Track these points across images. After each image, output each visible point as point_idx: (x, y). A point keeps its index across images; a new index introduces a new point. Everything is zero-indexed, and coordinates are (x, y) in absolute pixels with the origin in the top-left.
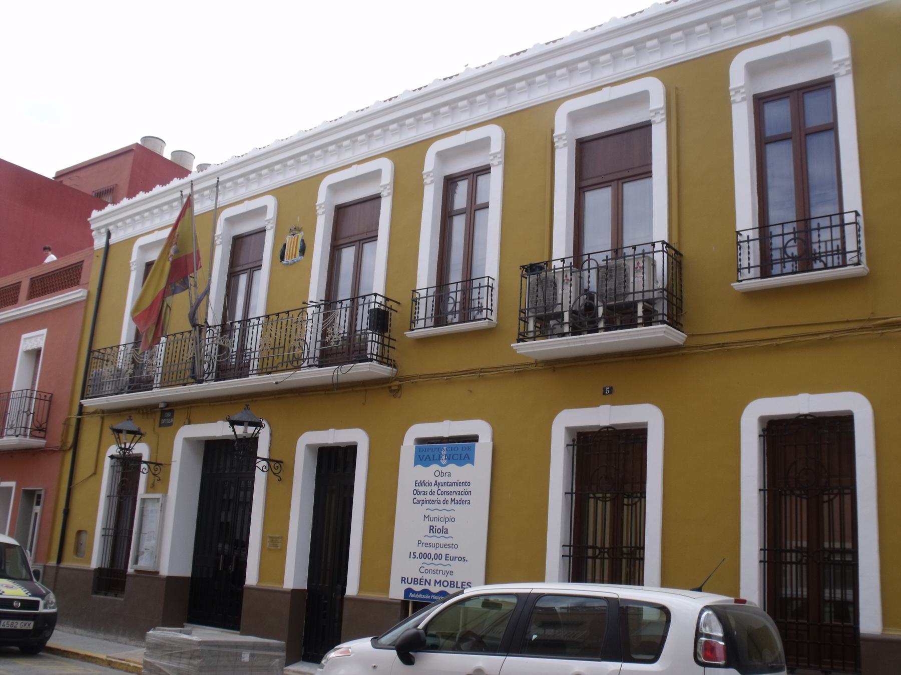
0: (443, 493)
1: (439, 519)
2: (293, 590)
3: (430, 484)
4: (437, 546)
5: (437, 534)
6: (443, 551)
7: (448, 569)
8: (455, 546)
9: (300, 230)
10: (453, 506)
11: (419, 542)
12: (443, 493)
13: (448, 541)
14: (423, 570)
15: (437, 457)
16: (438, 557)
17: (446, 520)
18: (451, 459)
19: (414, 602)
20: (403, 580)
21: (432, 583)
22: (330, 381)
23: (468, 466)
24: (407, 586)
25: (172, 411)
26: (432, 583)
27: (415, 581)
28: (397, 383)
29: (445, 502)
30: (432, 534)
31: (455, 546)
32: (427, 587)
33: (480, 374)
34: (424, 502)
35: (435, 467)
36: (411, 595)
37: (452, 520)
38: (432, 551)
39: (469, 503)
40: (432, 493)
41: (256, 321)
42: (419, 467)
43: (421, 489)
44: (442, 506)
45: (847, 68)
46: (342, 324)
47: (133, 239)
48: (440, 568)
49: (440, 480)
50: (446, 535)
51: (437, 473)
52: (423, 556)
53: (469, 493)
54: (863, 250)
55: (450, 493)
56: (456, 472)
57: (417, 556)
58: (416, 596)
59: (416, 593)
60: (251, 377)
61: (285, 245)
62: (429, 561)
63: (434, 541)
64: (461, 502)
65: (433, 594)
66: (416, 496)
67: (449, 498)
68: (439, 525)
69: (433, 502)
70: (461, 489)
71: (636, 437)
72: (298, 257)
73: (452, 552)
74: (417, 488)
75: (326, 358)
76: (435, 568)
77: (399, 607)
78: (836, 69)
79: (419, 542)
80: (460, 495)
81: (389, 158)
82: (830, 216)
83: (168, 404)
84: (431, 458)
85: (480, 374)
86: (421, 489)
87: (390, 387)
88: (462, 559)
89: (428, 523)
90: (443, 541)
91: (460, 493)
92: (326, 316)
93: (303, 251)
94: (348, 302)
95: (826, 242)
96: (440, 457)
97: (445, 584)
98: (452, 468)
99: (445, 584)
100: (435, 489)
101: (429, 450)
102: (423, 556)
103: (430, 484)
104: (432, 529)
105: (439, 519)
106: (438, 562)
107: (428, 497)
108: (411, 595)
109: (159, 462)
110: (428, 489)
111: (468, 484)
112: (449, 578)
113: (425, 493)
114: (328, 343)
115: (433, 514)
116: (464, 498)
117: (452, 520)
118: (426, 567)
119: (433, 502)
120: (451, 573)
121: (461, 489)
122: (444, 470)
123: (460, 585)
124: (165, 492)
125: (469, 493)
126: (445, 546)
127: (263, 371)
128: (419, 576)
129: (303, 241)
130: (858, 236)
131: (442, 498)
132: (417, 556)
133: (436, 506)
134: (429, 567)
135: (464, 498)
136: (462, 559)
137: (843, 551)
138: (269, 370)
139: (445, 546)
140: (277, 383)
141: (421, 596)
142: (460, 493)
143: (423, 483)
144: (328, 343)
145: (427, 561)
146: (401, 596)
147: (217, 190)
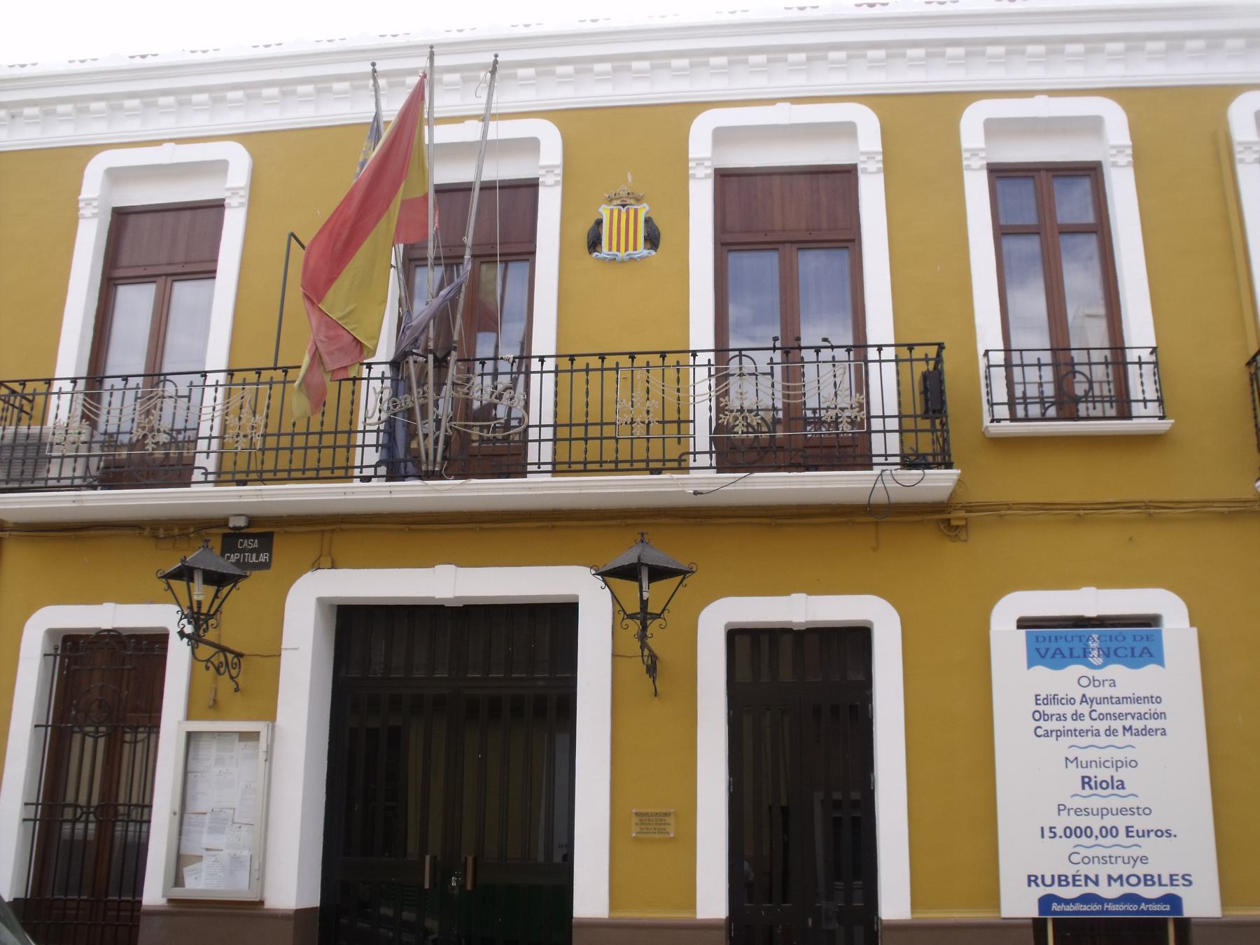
0: (1103, 717)
1: (1101, 764)
2: (299, 912)
3: (1071, 701)
4: (1102, 812)
5: (1100, 791)
6: (1121, 822)
7: (1135, 852)
8: (1147, 811)
9: (638, 200)
10: (1129, 739)
11: (1061, 808)
12: (1103, 717)
13: (1130, 803)
14: (1075, 858)
15: (1077, 653)
16: (1111, 832)
17: (1117, 765)
18: (1110, 656)
19: (1054, 920)
20: (1032, 880)
21: (1103, 880)
22: (862, 499)
23: (1152, 668)
24: (1043, 891)
25: (266, 541)
26: (1103, 880)
27: (1062, 880)
28: (962, 514)
29: (1111, 732)
30: (1088, 791)
31: (1147, 811)
32: (1091, 889)
33: (1149, 511)
34: (1060, 734)
35: (1076, 670)
36: (1055, 907)
37: (1133, 764)
38: (1095, 823)
39: (1164, 733)
40: (1077, 716)
41: (119, 383)
42: (1041, 671)
43: (1050, 709)
44: (1103, 740)
45: (1126, 158)
46: (207, 411)
47: (89, 151)
48: (1115, 852)
49: (1091, 692)
50: (1121, 792)
51: (1084, 682)
52: (1070, 832)
53: (1162, 715)
54: (985, 407)
55: (1120, 716)
56: (1125, 679)
57: (1060, 832)
58: (1069, 908)
59: (1067, 902)
60: (531, 478)
61: (599, 223)
62: (1092, 841)
63: (1095, 803)
64: (1147, 732)
65: (1108, 901)
66: (1041, 723)
67: (1117, 725)
68: (1103, 774)
69: (1082, 733)
70: (1143, 708)
71: (856, 640)
72: (642, 251)
73: (1139, 823)
74: (1041, 708)
75: (733, 453)
76: (1107, 852)
77: (1031, 932)
78: (1113, 156)
79: (1061, 808)
80: (1146, 720)
81: (558, 125)
82: (1088, 349)
83: (252, 520)
84: (1067, 653)
85: (1149, 511)
86: (1050, 709)
87: (949, 520)
88: (1160, 833)
89: (1076, 773)
90: (1115, 803)
91: (1141, 717)
92: (787, 375)
93: (653, 240)
94: (222, 378)
95: (1101, 383)
96: (1086, 653)
97: (1133, 880)
98: (1116, 671)
99: (1133, 880)
100: (1084, 709)
101: (1053, 638)
102: (1070, 832)
103: (1071, 701)
104: (1086, 782)
105: (1101, 764)
106: (1109, 840)
107: (1070, 724)
108: (1055, 907)
109: (224, 643)
110: (1068, 710)
111: (1159, 700)
112: (1141, 870)
113: (1061, 717)
114: (731, 429)
115: (1084, 756)
116: (1152, 724)
117: (1133, 764)
118: (1084, 852)
119: (1082, 733)
120: (1143, 860)
121: (1143, 708)
122: (1099, 674)
123: (1165, 880)
124: (270, 714)
125: (1162, 715)
126: (1122, 811)
127: (221, 477)
128: (1070, 871)
129: (648, 221)
130: (988, 385)
131: (1102, 725)
132: (1060, 832)
133: (1090, 740)
134: (1090, 853)
135: (1152, 724)
136: (1160, 833)
137: (855, 805)
138: (242, 477)
139: (1122, 811)
140: (696, 493)
141: (1155, 907)
142: (1141, 717)
143: (1053, 699)
144: (731, 429)
145: (1084, 840)
146: (1031, 910)
147: (376, 88)
